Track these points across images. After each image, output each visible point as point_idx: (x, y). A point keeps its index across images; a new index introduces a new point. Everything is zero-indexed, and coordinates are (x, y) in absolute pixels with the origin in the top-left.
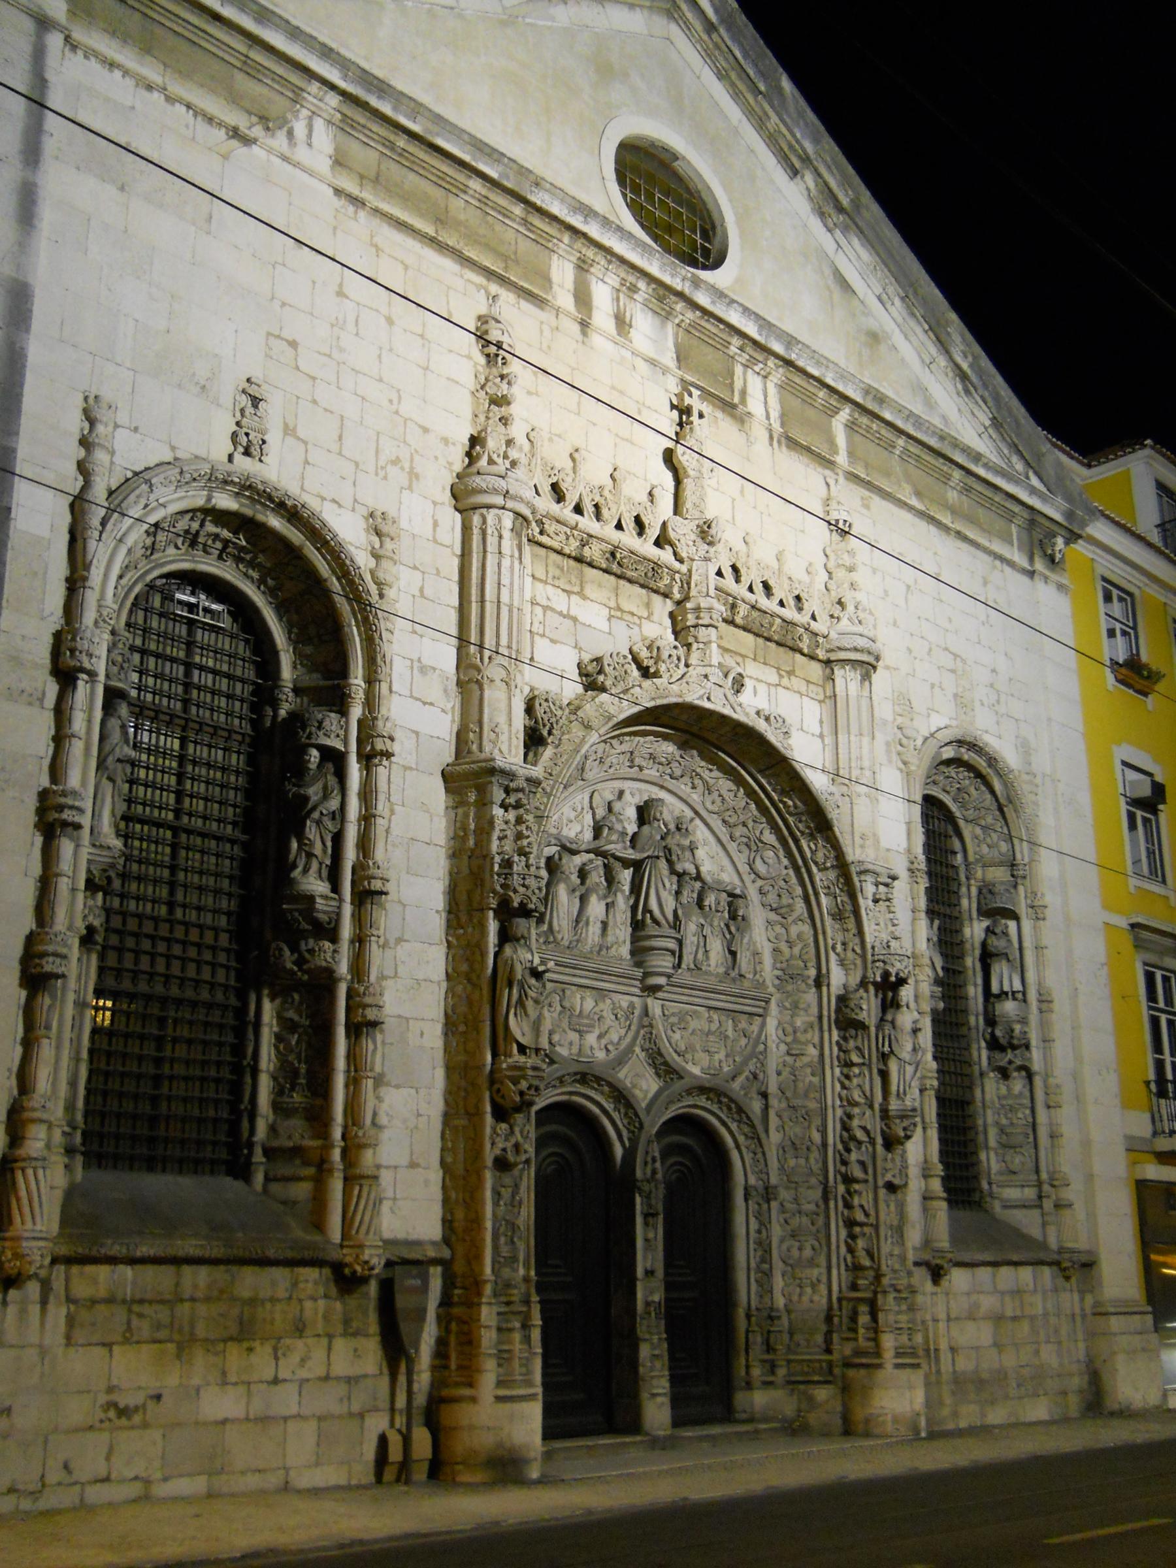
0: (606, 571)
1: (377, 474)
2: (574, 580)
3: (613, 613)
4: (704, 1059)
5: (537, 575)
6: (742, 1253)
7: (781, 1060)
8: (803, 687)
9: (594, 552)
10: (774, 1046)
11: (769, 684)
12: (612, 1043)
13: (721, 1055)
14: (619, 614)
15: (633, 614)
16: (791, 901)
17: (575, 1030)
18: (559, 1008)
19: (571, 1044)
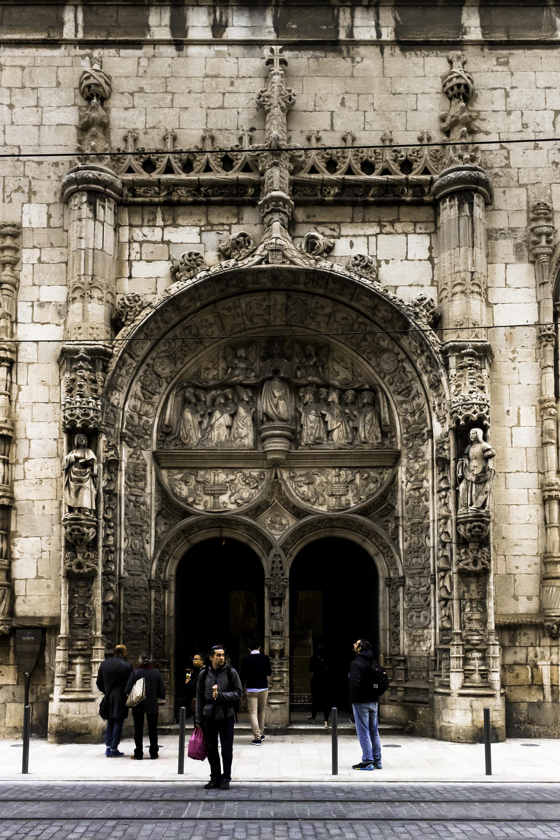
0: (195, 204)
1: (4, 201)
2: (166, 217)
3: (203, 229)
4: (332, 501)
5: (134, 223)
6: (384, 620)
7: (408, 494)
8: (410, 228)
9: (182, 194)
10: (404, 485)
11: (368, 236)
12: (242, 499)
13: (350, 496)
14: (209, 228)
15: (223, 224)
16: (408, 385)
17: (210, 495)
18: (194, 483)
19: (206, 502)
